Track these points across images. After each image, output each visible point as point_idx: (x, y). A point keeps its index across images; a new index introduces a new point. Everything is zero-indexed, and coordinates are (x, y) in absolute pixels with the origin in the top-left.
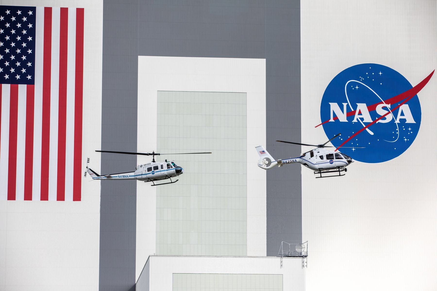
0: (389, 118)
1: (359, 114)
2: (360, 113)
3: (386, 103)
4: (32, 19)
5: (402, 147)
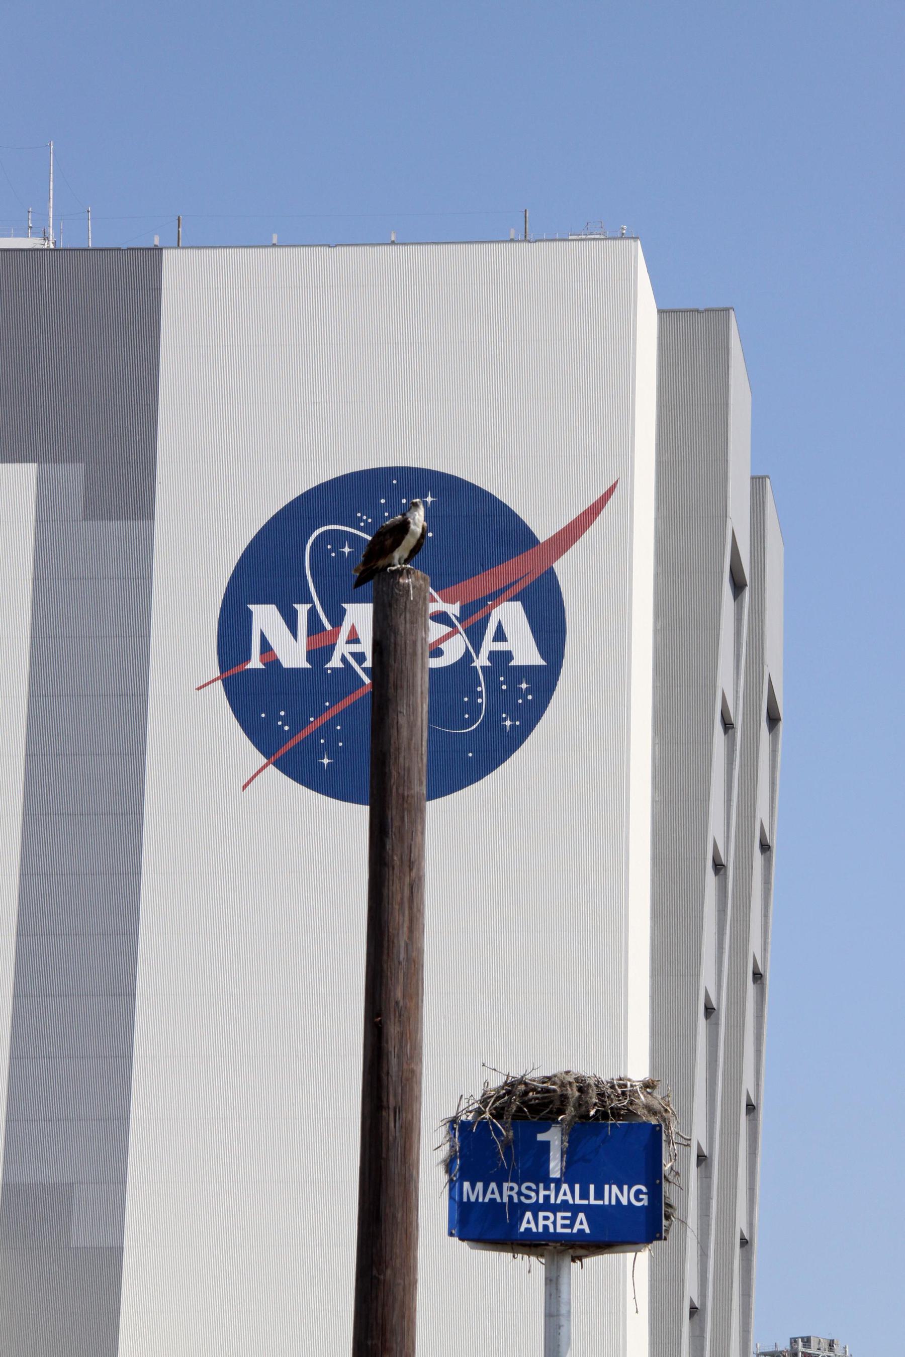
0: (455, 649)
1: (348, 642)
3: (445, 600)
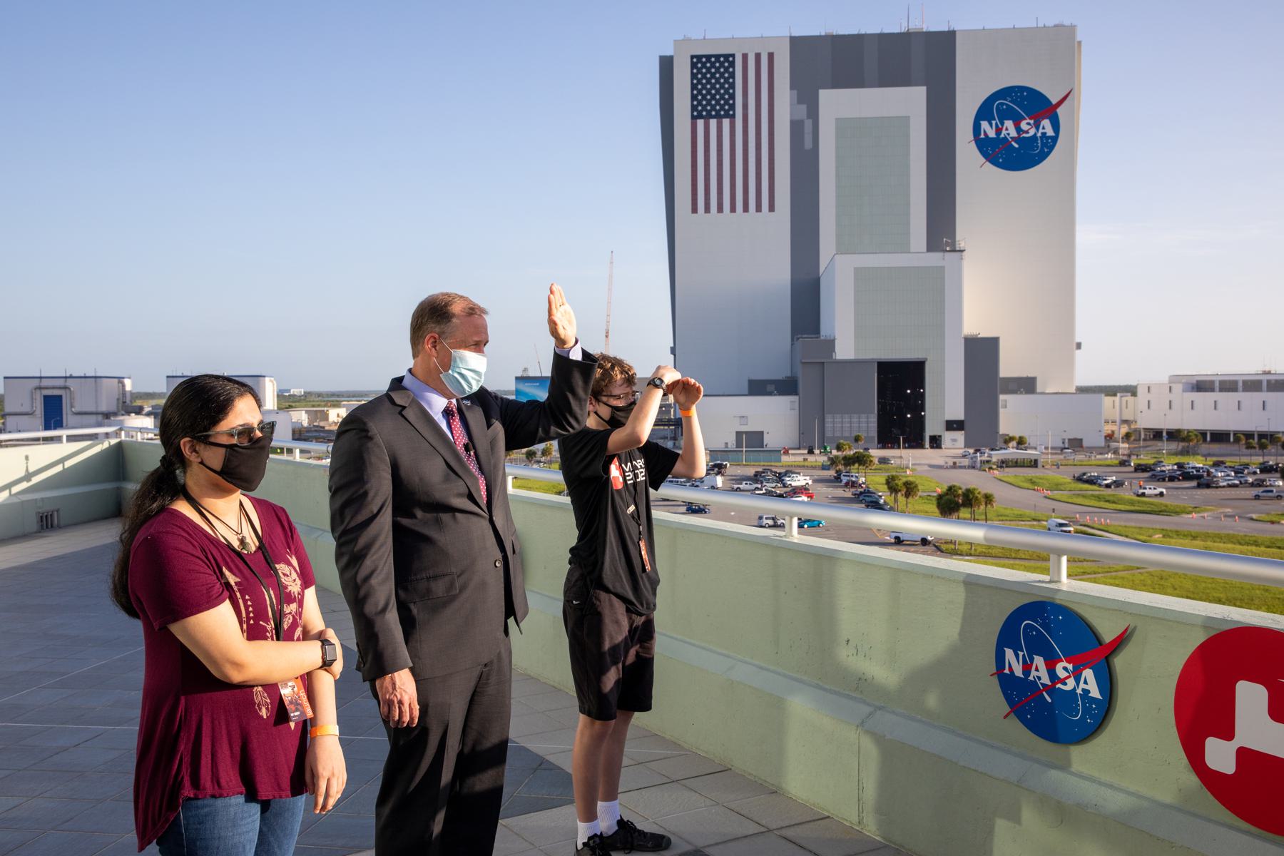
0: (1032, 132)
4: (732, 64)
5: (1043, 156)
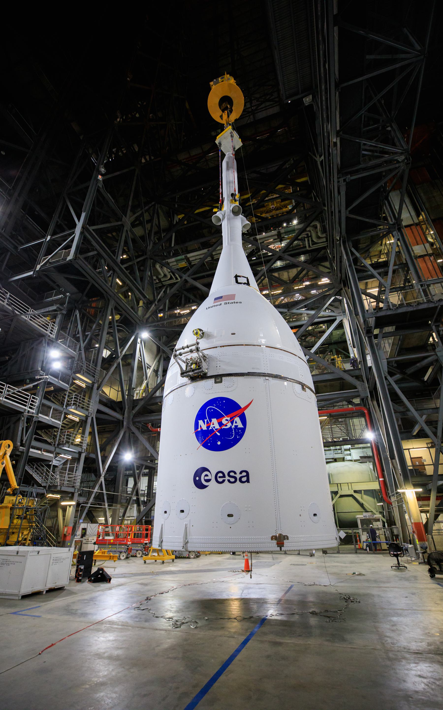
0: (229, 425)
2: (213, 424)
5: (236, 441)
